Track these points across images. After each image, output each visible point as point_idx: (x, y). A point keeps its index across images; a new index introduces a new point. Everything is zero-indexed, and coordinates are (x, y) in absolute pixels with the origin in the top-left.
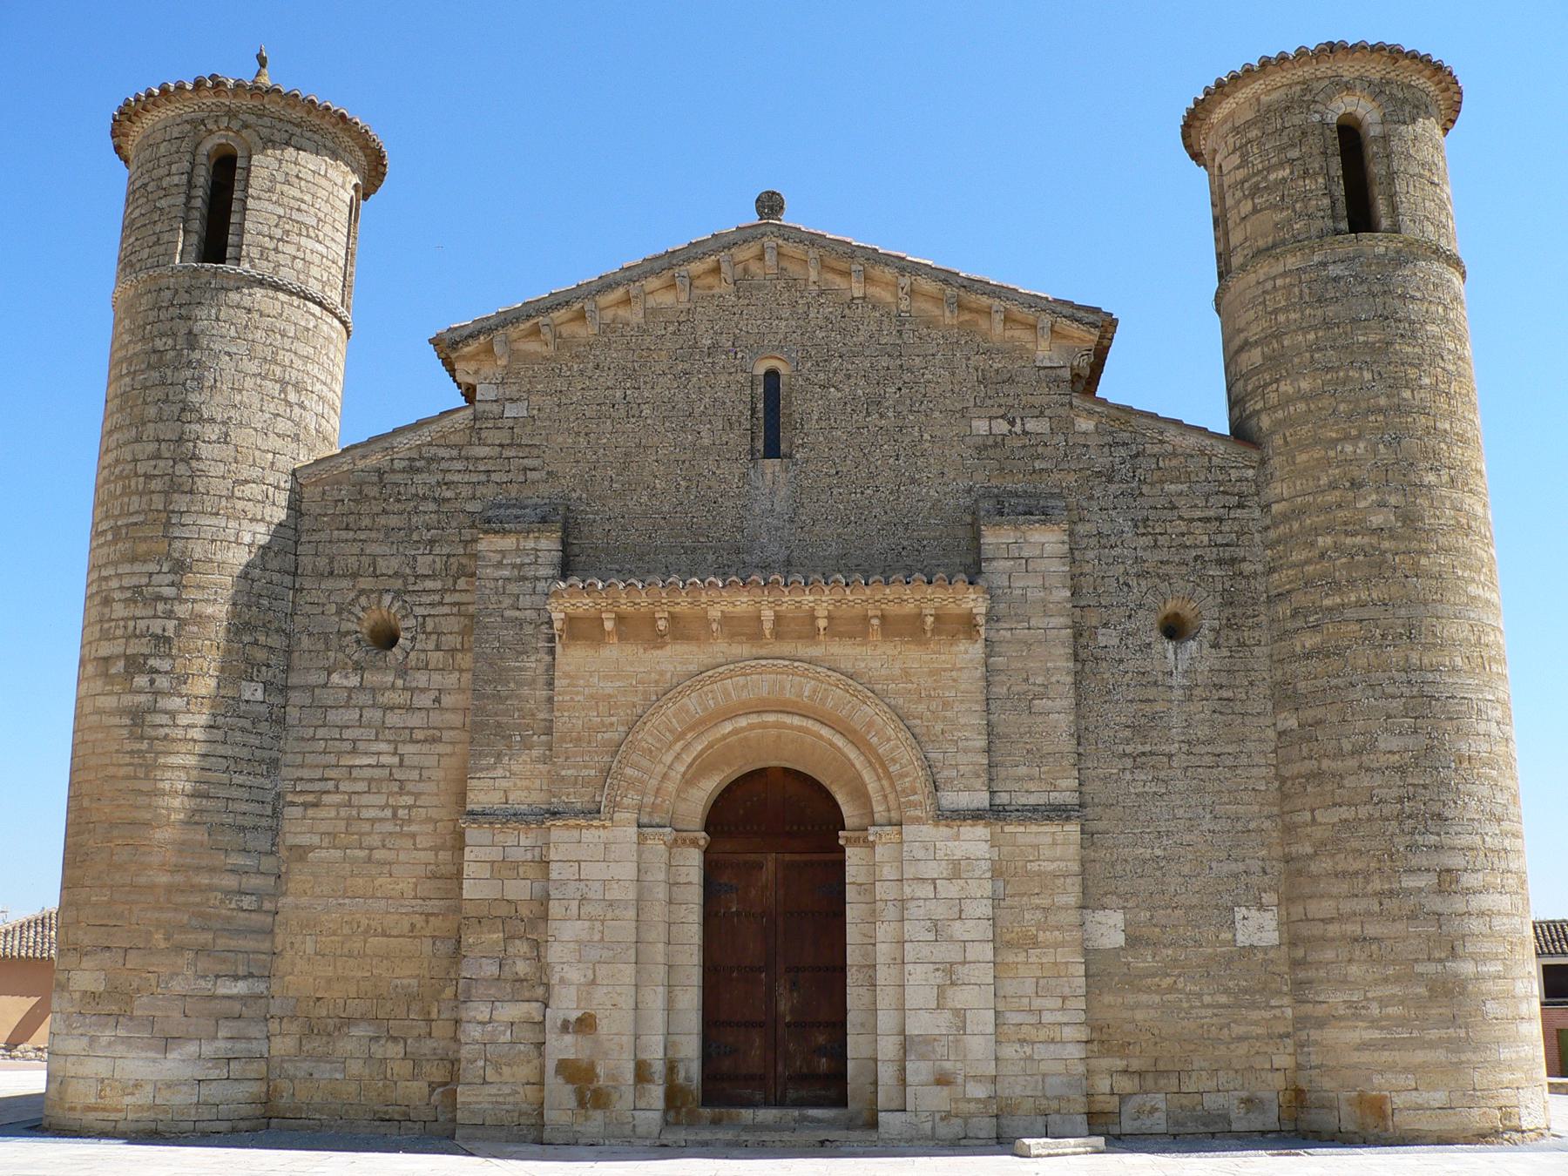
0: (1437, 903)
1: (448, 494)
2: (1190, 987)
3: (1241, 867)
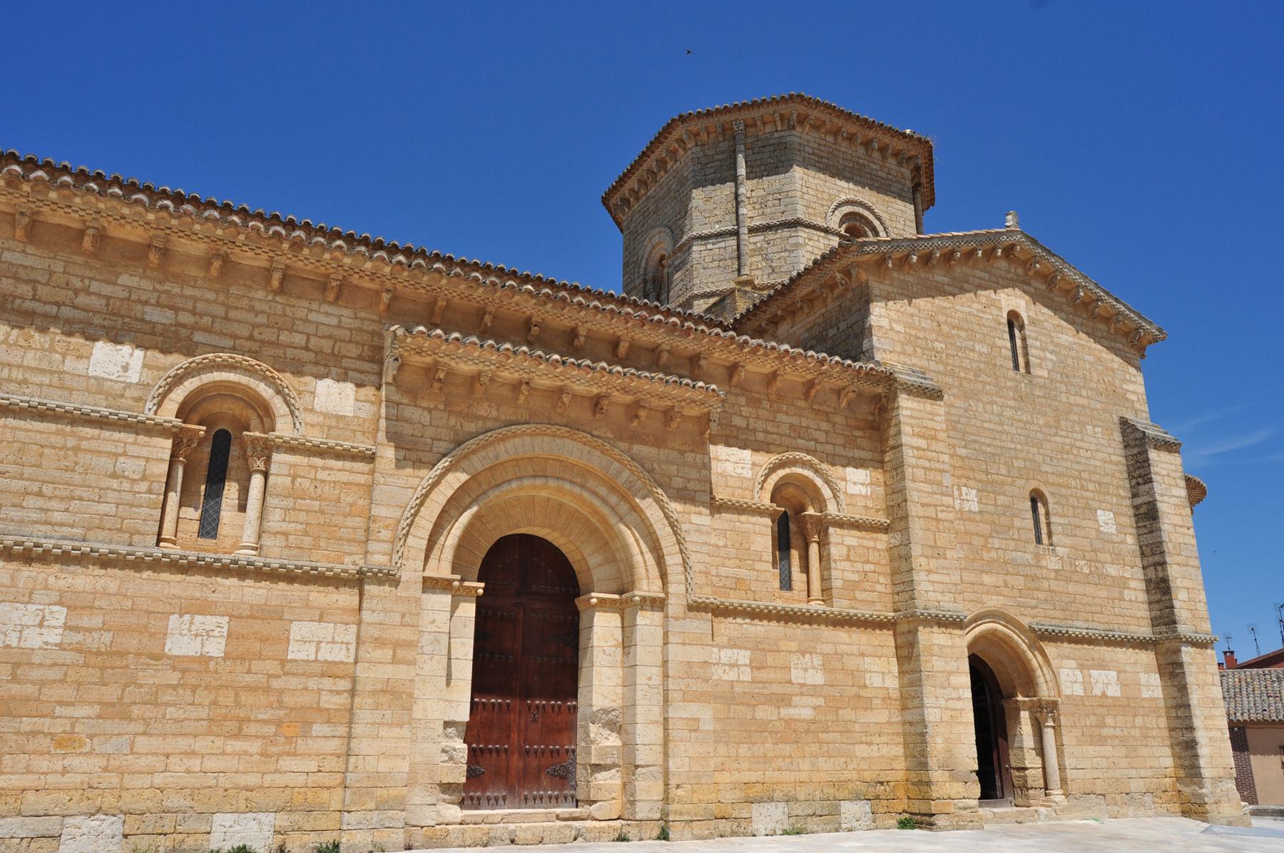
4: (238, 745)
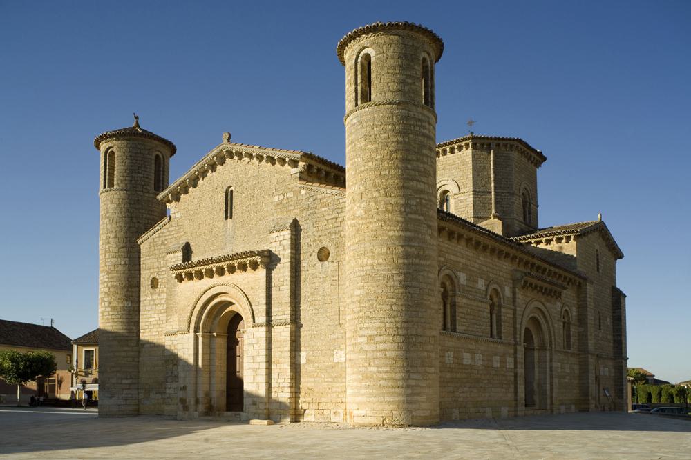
0: (366, 348)
3: (335, 336)
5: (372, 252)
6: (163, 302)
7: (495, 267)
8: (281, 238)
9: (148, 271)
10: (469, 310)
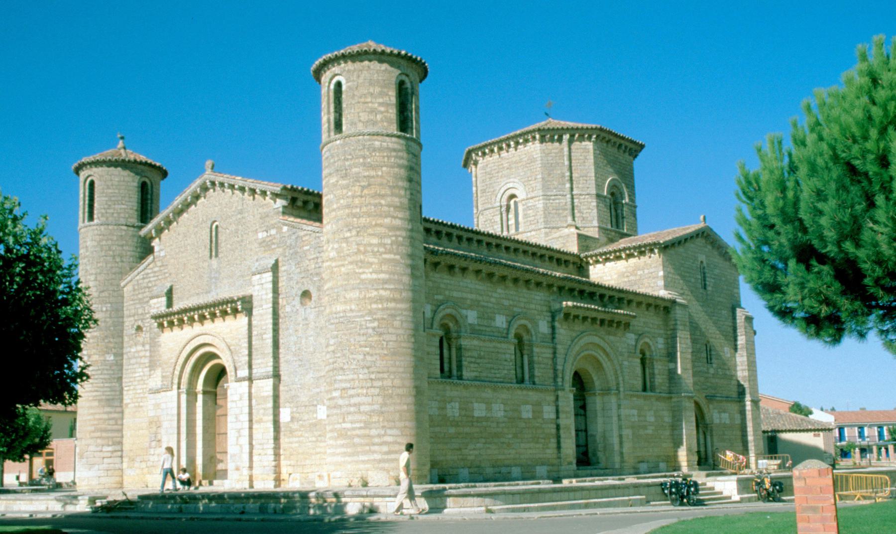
0: (340, 402)
1: (150, 285)
2: (306, 435)
3: (318, 390)
4: (537, 446)
5: (345, 298)
6: (148, 354)
7: (521, 299)
8: (263, 281)
9: (132, 319)
10: (482, 354)
